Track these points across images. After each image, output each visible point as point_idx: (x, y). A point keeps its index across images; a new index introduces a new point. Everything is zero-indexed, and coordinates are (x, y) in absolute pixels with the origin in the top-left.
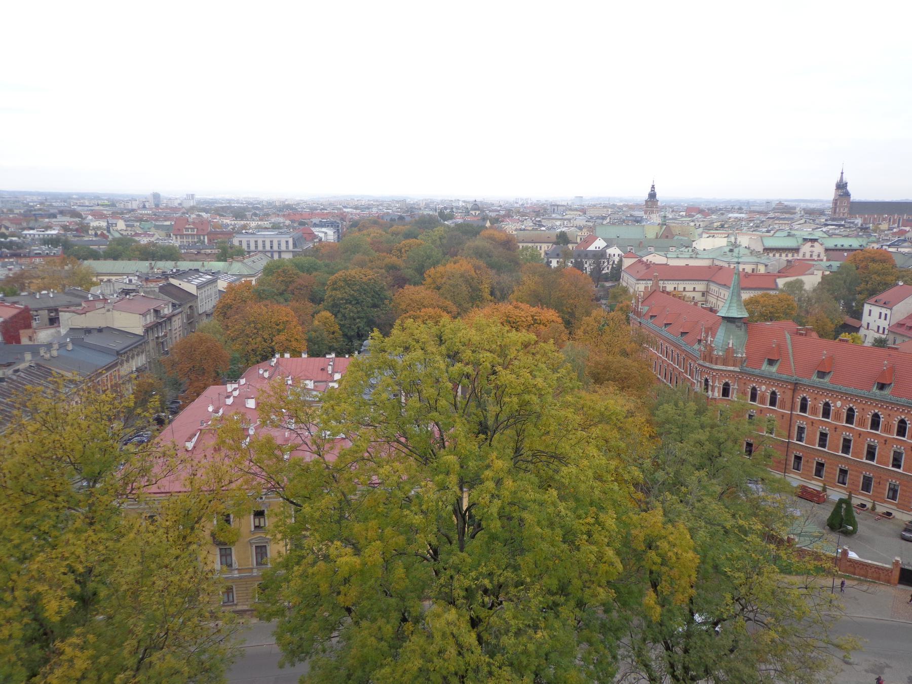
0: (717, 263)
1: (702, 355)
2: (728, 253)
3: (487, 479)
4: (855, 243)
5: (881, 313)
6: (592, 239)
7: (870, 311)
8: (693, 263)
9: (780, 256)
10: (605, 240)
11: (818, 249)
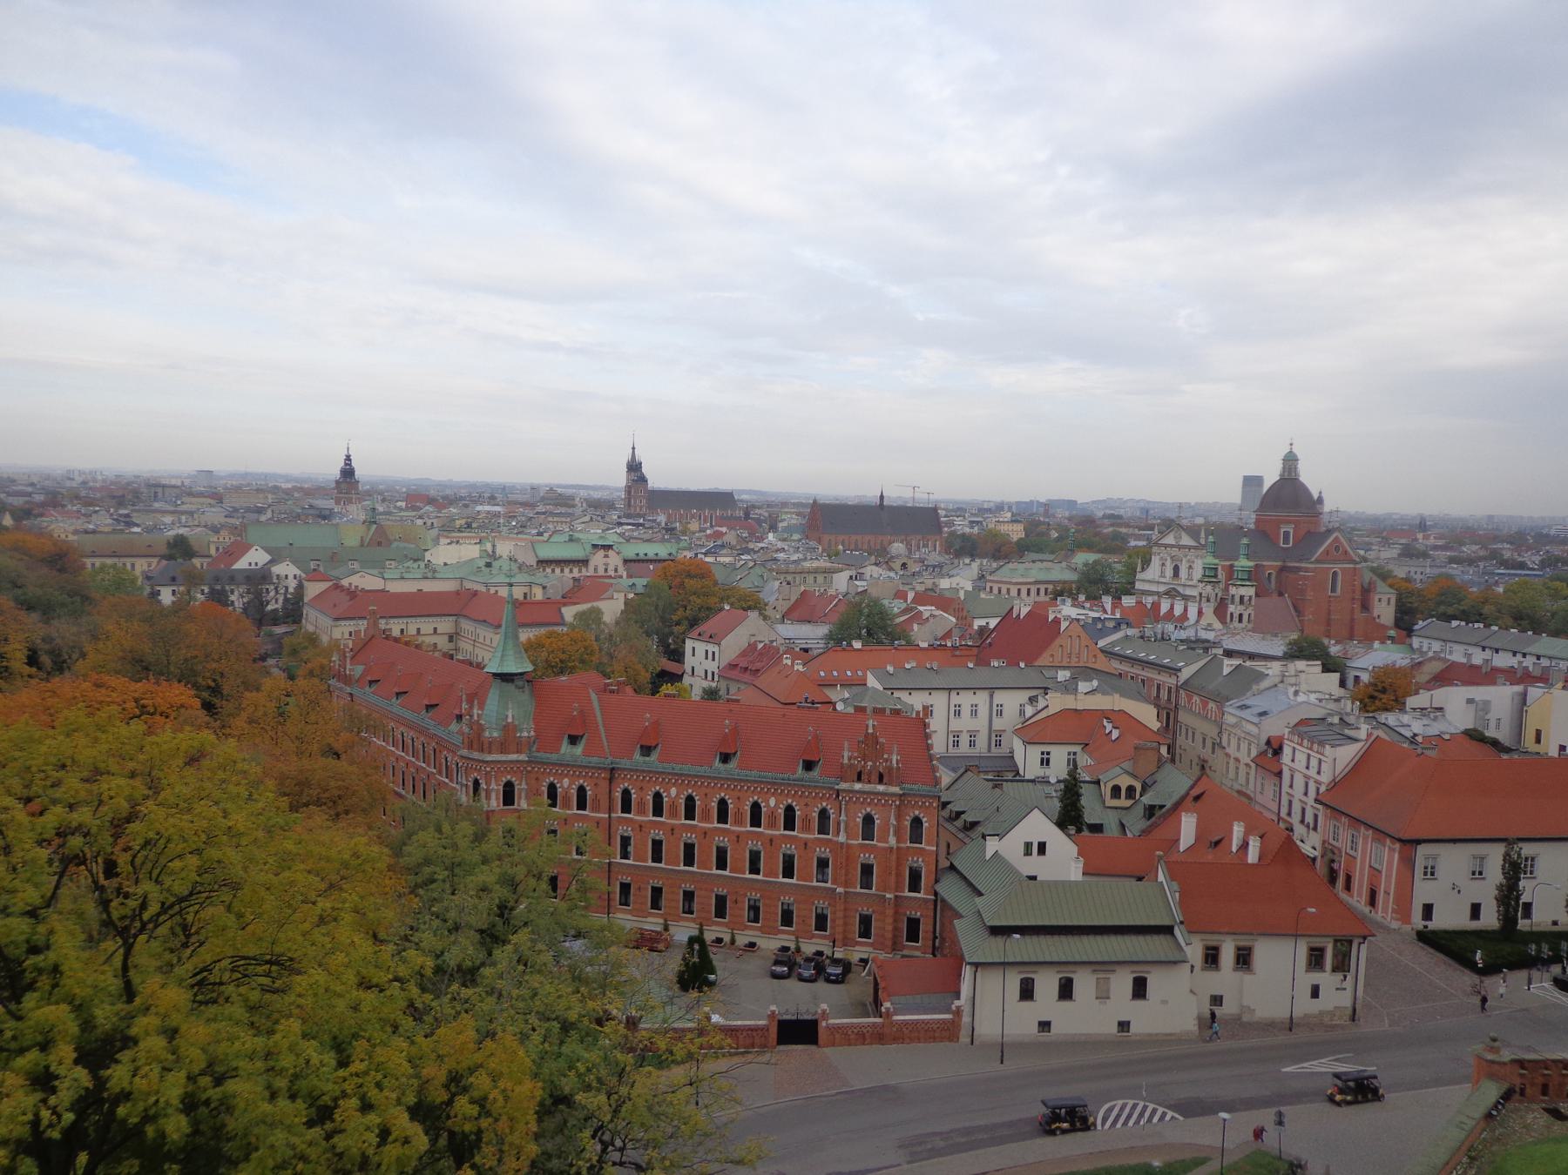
0: (468, 585)
1: (466, 741)
2: (483, 568)
3: (147, 1033)
4: (662, 550)
5: (707, 651)
6: (241, 549)
7: (694, 648)
8: (429, 586)
9: (562, 571)
10: (267, 550)
11: (614, 560)
